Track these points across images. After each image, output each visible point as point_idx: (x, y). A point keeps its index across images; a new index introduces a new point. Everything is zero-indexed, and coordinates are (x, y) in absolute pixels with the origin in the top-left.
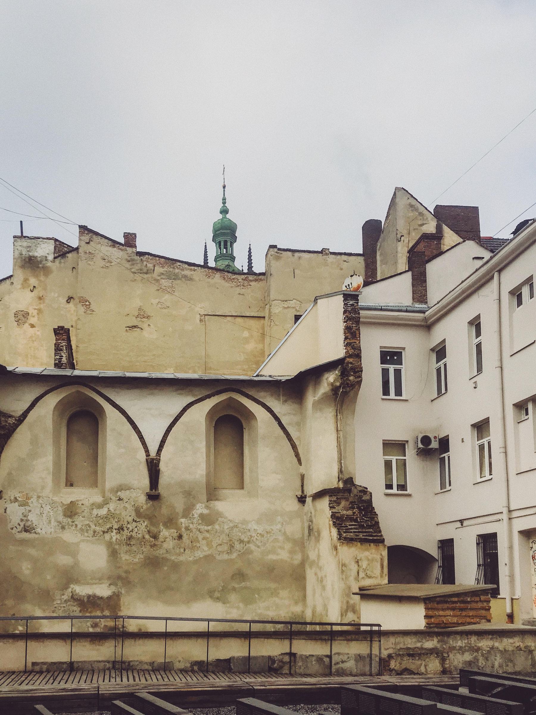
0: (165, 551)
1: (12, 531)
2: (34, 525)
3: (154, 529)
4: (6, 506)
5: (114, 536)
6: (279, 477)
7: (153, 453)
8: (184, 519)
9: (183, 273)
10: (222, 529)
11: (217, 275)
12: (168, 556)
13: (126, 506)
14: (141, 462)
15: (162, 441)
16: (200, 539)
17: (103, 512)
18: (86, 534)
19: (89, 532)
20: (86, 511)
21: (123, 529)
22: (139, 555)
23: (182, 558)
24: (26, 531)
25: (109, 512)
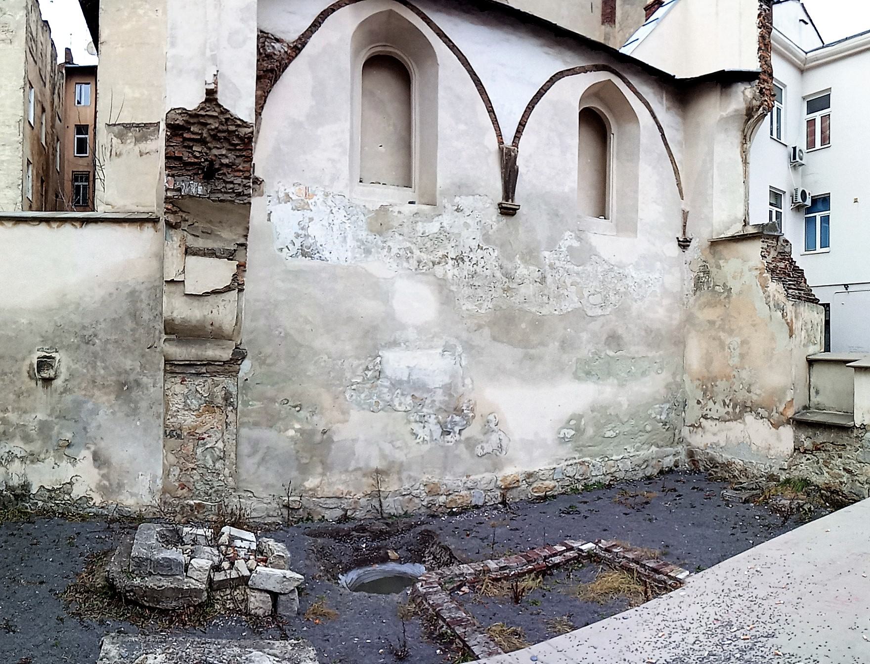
1: (279, 253)
2: (318, 244)
3: (509, 266)
4: (271, 208)
5: (450, 270)
8: (549, 253)
10: (594, 272)
13: (468, 222)
14: (490, 152)
16: (569, 285)
17: (433, 228)
18: (405, 265)
19: (411, 260)
20: (405, 225)
21: (463, 260)
22: (486, 303)
24: (304, 255)
25: (442, 229)
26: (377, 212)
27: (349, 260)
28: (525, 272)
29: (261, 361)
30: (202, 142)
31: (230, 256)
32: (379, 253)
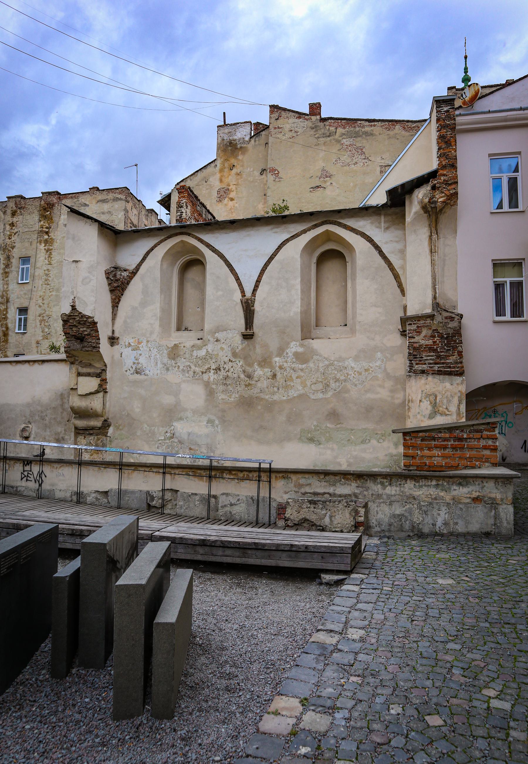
0: (259, 391)
3: (249, 370)
4: (122, 350)
5: (212, 376)
6: (380, 310)
7: (248, 294)
9: (363, 130)
10: (316, 367)
11: (397, 127)
12: (262, 396)
14: (237, 303)
15: (257, 281)
16: (294, 378)
18: (187, 375)
19: (190, 372)
20: (187, 353)
21: (220, 370)
22: (234, 395)
23: (276, 397)
26: (172, 348)
27: (159, 375)
28: (261, 373)
29: (117, 428)
30: (75, 326)
31: (98, 375)
32: (173, 370)
